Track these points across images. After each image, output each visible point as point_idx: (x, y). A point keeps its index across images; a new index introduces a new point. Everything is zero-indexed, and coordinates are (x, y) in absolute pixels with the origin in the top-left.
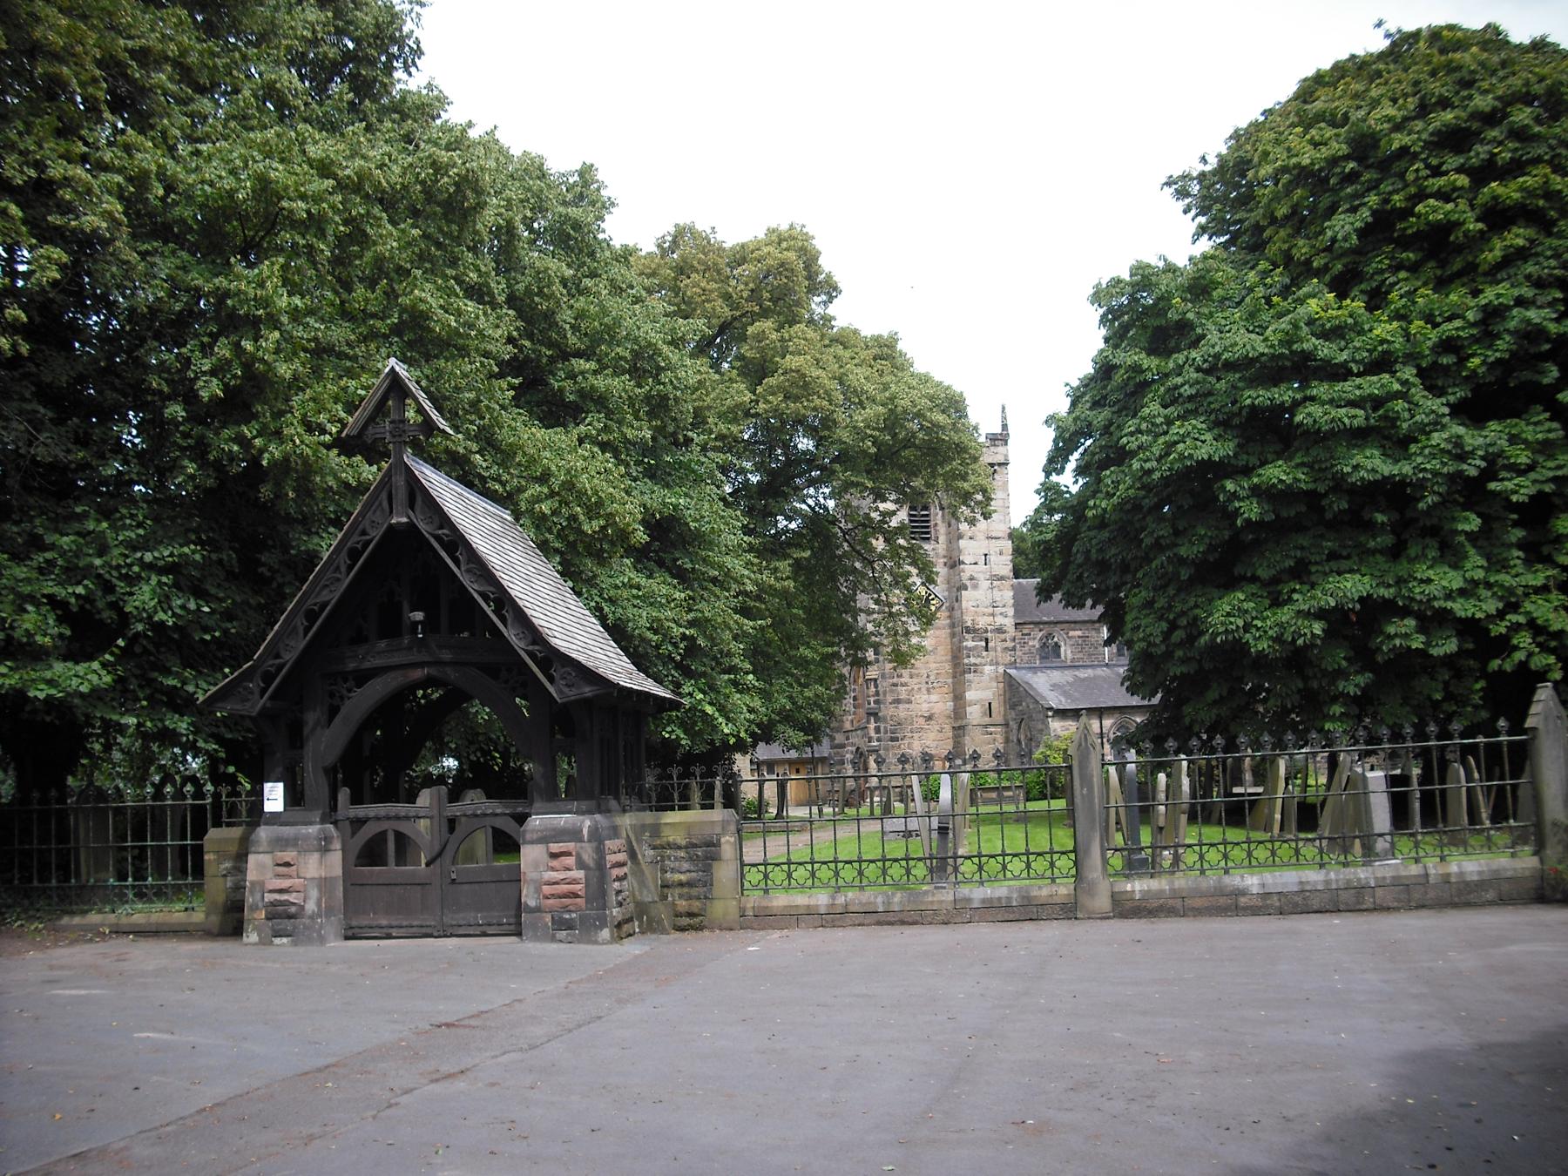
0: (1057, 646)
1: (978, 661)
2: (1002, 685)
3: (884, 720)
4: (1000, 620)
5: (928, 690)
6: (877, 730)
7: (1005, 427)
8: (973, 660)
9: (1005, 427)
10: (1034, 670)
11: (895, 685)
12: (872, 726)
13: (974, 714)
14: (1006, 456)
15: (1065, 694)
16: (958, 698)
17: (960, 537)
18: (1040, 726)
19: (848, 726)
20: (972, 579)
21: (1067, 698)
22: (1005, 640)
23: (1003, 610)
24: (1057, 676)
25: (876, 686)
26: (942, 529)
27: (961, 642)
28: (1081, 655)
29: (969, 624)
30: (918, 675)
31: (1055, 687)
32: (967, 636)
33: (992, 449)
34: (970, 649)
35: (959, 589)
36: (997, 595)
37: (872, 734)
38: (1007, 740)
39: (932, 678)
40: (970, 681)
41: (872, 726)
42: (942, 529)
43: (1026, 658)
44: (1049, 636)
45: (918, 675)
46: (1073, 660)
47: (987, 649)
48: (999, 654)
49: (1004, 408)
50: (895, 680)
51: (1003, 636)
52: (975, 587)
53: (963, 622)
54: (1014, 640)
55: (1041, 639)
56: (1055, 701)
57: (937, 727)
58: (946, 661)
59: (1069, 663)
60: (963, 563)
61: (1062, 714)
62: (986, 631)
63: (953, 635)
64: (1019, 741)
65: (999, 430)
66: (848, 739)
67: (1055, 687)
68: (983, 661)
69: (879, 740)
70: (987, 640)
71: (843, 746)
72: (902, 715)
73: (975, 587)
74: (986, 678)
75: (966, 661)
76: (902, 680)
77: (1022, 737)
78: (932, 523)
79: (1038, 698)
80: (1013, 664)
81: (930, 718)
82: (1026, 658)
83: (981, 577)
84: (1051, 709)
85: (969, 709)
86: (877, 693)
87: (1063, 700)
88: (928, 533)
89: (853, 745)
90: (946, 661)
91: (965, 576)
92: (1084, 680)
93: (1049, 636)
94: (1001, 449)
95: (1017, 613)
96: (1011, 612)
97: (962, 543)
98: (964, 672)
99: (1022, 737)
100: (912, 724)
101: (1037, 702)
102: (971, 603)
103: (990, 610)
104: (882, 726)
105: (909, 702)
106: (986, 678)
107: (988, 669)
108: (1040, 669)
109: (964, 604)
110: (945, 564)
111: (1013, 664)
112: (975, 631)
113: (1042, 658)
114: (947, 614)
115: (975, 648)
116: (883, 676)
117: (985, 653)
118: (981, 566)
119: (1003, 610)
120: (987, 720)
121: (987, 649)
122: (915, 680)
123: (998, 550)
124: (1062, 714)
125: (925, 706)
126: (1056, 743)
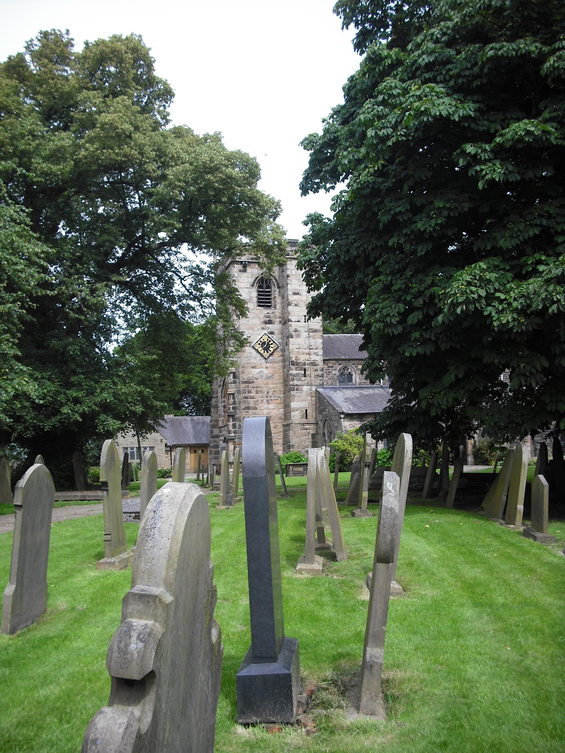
0: (350, 375)
4: (313, 357)
5: (268, 401)
6: (234, 426)
8: (296, 382)
10: (335, 389)
12: (231, 423)
13: (296, 416)
15: (353, 404)
16: (287, 406)
17: (289, 304)
18: (336, 425)
20: (296, 331)
21: (354, 407)
22: (317, 370)
23: (316, 351)
24: (349, 393)
25: (234, 398)
26: (279, 300)
27: (288, 371)
29: (294, 359)
30: (261, 392)
31: (347, 399)
32: (292, 367)
34: (294, 375)
35: (288, 338)
36: (312, 341)
37: (231, 428)
39: (270, 393)
41: (231, 423)
42: (279, 300)
43: (330, 382)
44: (345, 368)
45: (261, 392)
46: (360, 384)
47: (305, 375)
48: (313, 379)
50: (246, 395)
51: (315, 368)
52: (298, 336)
53: (290, 358)
54: (322, 370)
55: (340, 370)
56: (347, 408)
58: (280, 383)
60: (291, 321)
61: (350, 416)
62: (305, 364)
63: (284, 367)
64: (324, 434)
66: (221, 432)
67: (347, 399)
68: (302, 383)
69: (235, 432)
70: (305, 370)
71: (218, 436)
73: (298, 336)
74: (304, 394)
75: (291, 383)
76: (251, 394)
77: (326, 432)
78: (273, 296)
79: (335, 406)
82: (330, 382)
83: (302, 330)
84: (343, 413)
85: (293, 414)
86: (234, 403)
87: (351, 407)
88: (270, 302)
89: (223, 435)
90: (280, 383)
91: (292, 329)
92: (366, 396)
93: (345, 368)
95: (325, 353)
96: (321, 352)
97: (290, 308)
98: (290, 390)
99: (326, 432)
101: (334, 409)
102: (295, 346)
104: (237, 423)
105: (255, 408)
106: (304, 394)
107: (305, 388)
108: (339, 389)
109: (291, 347)
110: (280, 322)
111: (322, 385)
112: (298, 364)
113: (340, 382)
114: (281, 353)
115: (297, 374)
116: (239, 392)
117: (303, 378)
119: (316, 351)
120: (304, 420)
121: (305, 375)
122: (259, 395)
124: (350, 416)
125: (266, 411)
126: (345, 435)
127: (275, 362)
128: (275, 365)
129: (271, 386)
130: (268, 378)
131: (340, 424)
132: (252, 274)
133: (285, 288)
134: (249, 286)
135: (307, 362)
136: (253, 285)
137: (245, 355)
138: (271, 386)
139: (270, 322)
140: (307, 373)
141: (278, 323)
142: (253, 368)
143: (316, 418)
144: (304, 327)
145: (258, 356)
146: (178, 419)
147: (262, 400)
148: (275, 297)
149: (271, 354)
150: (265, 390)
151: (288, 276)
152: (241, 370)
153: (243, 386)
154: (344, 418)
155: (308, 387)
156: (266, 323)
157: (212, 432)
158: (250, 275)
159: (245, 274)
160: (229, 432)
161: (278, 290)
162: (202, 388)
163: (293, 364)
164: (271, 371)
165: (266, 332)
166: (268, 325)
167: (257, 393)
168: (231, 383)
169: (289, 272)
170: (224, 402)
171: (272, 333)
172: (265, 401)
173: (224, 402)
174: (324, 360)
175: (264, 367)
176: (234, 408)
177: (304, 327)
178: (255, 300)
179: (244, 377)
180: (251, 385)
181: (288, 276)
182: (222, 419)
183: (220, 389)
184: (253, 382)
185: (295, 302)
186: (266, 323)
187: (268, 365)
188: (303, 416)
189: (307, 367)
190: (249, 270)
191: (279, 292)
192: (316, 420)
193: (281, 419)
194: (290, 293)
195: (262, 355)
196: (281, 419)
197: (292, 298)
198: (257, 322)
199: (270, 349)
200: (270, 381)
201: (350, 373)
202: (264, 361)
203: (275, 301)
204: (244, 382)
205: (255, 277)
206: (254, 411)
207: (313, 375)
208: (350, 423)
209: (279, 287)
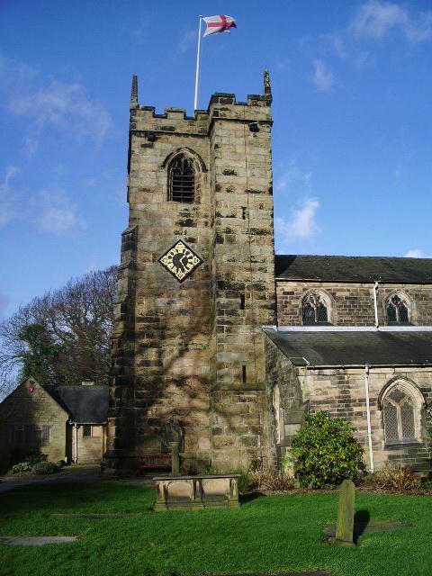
4: (257, 276)
7: (268, 89)
9: (268, 89)
20: (228, 231)
22: (263, 298)
23: (262, 265)
33: (254, 108)
47: (242, 307)
51: (262, 293)
62: (242, 287)
65: (261, 93)
70: (243, 298)
83: (239, 230)
103: (247, 265)
110: (206, 224)
112: (230, 286)
115: (228, 305)
117: (240, 311)
118: (239, 219)
121: (242, 307)
132: (162, 151)
136: (163, 166)
139: (189, 223)
141: (203, 225)
156: (182, 224)
159: (149, 151)
166: (185, 228)
171: (192, 240)
179: (142, 308)
185: (227, 186)
186: (182, 224)
189: (246, 291)
190: (157, 145)
199: (188, 265)
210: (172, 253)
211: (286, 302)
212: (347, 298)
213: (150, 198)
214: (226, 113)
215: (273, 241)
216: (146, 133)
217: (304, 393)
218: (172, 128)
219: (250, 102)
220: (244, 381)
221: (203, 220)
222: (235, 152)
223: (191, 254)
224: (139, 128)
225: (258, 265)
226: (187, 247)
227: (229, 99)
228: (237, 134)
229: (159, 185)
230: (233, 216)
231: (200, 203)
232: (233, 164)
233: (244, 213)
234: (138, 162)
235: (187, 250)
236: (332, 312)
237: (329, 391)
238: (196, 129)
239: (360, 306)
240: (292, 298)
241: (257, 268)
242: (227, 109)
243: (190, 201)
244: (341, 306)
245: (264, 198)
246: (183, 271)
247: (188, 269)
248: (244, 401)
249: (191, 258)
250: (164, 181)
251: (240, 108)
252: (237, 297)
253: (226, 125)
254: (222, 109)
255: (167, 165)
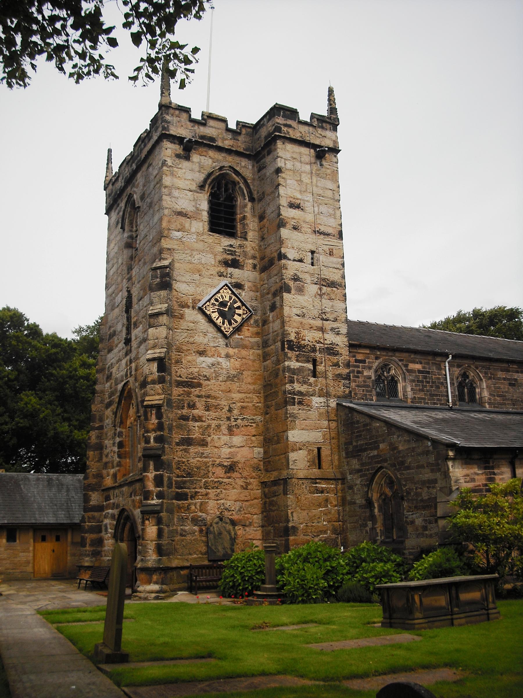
0: (393, 382)
1: (303, 388)
2: (333, 425)
3: (168, 466)
4: (330, 338)
6: (158, 481)
7: (333, 110)
8: (297, 387)
11: (185, 418)
12: (151, 475)
14: (336, 142)
18: (427, 475)
19: (108, 482)
20: (296, 279)
22: (337, 365)
23: (335, 325)
25: (159, 416)
26: (252, 224)
27: (278, 362)
28: (421, 395)
29: (292, 337)
30: (217, 407)
32: (290, 354)
33: (320, 131)
34: (293, 371)
36: (327, 304)
37: (151, 486)
38: (343, 502)
39: (236, 412)
40: (294, 417)
41: (151, 475)
42: (252, 224)
43: (360, 391)
44: (385, 367)
45: (217, 407)
46: (414, 400)
47: (314, 374)
48: (331, 383)
49: (331, 92)
50: (185, 411)
51: (335, 359)
52: (300, 290)
53: (284, 334)
57: (240, 482)
58: (255, 392)
59: (409, 404)
60: (285, 257)
62: (314, 350)
63: (265, 357)
64: (369, 504)
66: (107, 498)
69: (160, 496)
70: (315, 362)
71: (100, 508)
72: (194, 461)
73: (300, 290)
75: (288, 387)
76: (195, 412)
77: (375, 496)
80: (348, 397)
81: (231, 468)
84: (452, 446)
85: (292, 456)
86: (160, 427)
89: (114, 506)
90: (255, 392)
91: (288, 274)
93: (385, 367)
94: (329, 134)
97: (285, 232)
98: (286, 403)
99: (375, 496)
100: (206, 475)
102: (295, 311)
103: (318, 323)
105: (204, 443)
106: (314, 414)
109: (286, 310)
110: (255, 266)
112: (300, 347)
113: (378, 395)
114: (254, 330)
115: (300, 370)
116: (169, 402)
117: (312, 380)
118: (306, 266)
119: (335, 325)
120: (315, 472)
121: (314, 374)
122: (212, 414)
123: (326, 248)
125: (225, 451)
127: (244, 347)
128: (244, 353)
129: (237, 396)
130: (230, 378)
131: (446, 475)
132: (201, 167)
133: (267, 199)
134: (194, 187)
135: (318, 346)
136: (202, 187)
137: (184, 324)
138: (237, 396)
139: (235, 264)
140: (320, 368)
141: (250, 267)
142: (202, 353)
143: (339, 466)
144: (312, 275)
145: (211, 329)
146: (12, 478)
147: (219, 426)
148: (244, 218)
149: (238, 330)
150: (223, 403)
151: (278, 171)
152: (174, 355)
153: (177, 391)
154: (454, 459)
155: (322, 400)
156: (226, 264)
157: (86, 499)
158: (196, 167)
159: (185, 164)
160: (147, 495)
161: (250, 205)
162: (55, 429)
163: (291, 348)
164: (237, 364)
165: (224, 281)
166: (230, 270)
167: (208, 408)
168: (153, 382)
169: (280, 163)
170: (120, 434)
171: (239, 286)
172: (224, 428)
173: (120, 434)
174: (351, 346)
175: (223, 353)
176: (159, 439)
177: (312, 275)
178: (205, 216)
180: (196, 391)
181: (278, 171)
182: (112, 471)
183: (109, 412)
184: (199, 385)
187: (231, 351)
188: (312, 464)
189: (318, 355)
190: (195, 157)
191: (253, 208)
192: (342, 473)
193: (256, 468)
194: (283, 202)
195: (218, 329)
196: (256, 468)
197: (287, 213)
198: (209, 259)
199: (236, 317)
200: (235, 386)
201: (393, 377)
202: (222, 341)
203: (244, 225)
204: (180, 384)
205: (206, 173)
206: (200, 449)
207: (330, 375)
208: (465, 471)
209: (252, 199)
210: (217, 300)
211: (358, 372)
212: (420, 371)
213: (187, 225)
214: (290, 130)
215: (345, 295)
216: (180, 140)
217: (453, 479)
218: (212, 139)
219: (315, 123)
220: (319, 468)
221: (251, 261)
222: (301, 181)
223: (239, 304)
224: (173, 131)
225: (328, 325)
226: (233, 293)
227: (292, 113)
228: (302, 159)
229: (197, 209)
230: (301, 261)
231: (246, 239)
232: (299, 196)
233: (312, 259)
234: (172, 174)
235: (234, 297)
236: (404, 388)
237: (476, 477)
238: (241, 144)
239: (433, 382)
240: (364, 368)
241: (330, 327)
242: (289, 126)
243: (232, 235)
244: (413, 381)
245: (334, 241)
246: (230, 324)
247: (236, 322)
248: (322, 492)
249: (239, 308)
250: (205, 206)
251: (304, 129)
252: (308, 361)
253: (290, 147)
254: (286, 125)
255: (207, 186)
